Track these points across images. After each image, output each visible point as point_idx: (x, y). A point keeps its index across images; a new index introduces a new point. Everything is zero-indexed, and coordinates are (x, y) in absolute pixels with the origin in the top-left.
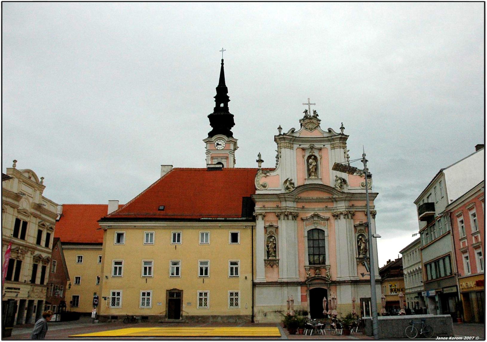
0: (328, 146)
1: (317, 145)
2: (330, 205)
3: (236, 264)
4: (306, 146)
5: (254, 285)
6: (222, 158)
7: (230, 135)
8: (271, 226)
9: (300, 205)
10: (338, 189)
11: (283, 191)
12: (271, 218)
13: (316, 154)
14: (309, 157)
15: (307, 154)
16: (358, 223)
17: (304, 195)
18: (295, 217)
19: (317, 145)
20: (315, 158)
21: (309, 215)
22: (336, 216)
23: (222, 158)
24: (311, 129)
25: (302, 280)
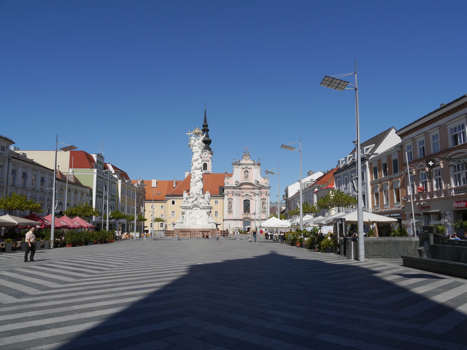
0: (253, 167)
1: (249, 167)
2: (253, 191)
3: (217, 212)
4: (244, 167)
5: (224, 220)
6: (207, 161)
7: (210, 149)
8: (230, 199)
9: (241, 191)
10: (256, 185)
11: (235, 186)
12: (230, 196)
13: (248, 170)
14: (245, 171)
15: (245, 170)
16: (262, 198)
17: (242, 187)
18: (239, 195)
19: (249, 167)
20: (248, 172)
21: (244, 194)
22: (255, 194)
23: (207, 161)
24: (247, 160)
25: (241, 218)
